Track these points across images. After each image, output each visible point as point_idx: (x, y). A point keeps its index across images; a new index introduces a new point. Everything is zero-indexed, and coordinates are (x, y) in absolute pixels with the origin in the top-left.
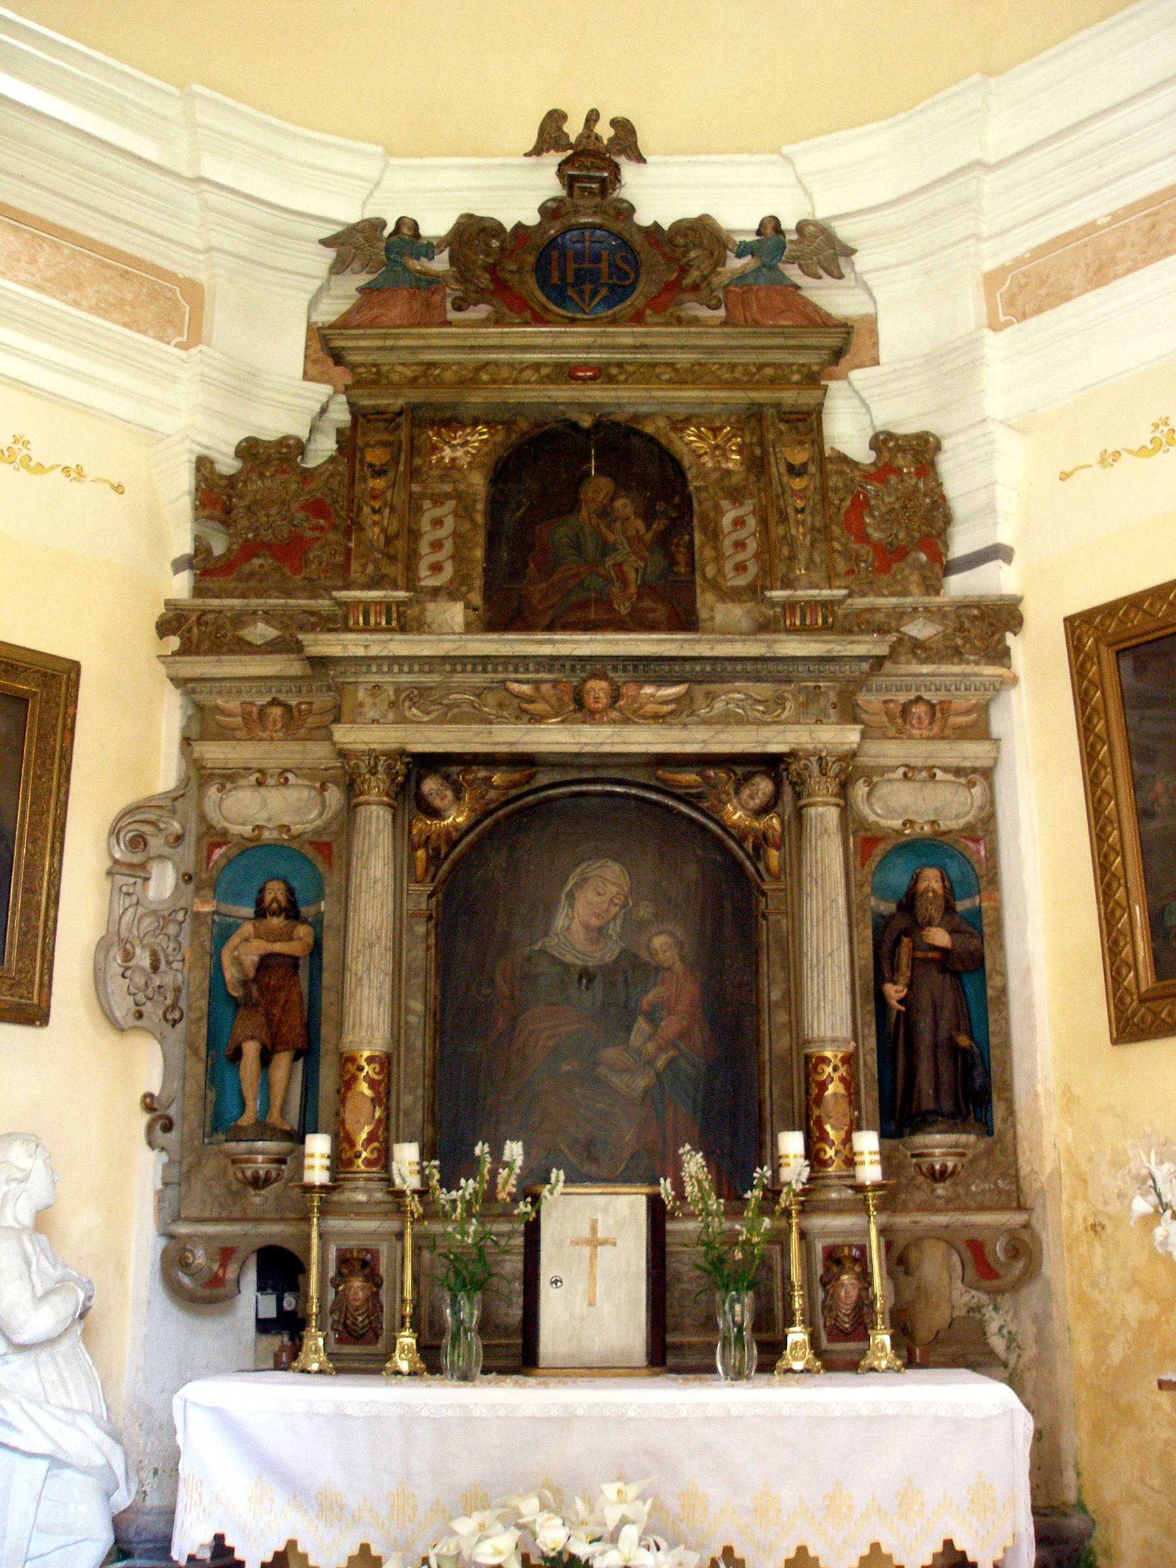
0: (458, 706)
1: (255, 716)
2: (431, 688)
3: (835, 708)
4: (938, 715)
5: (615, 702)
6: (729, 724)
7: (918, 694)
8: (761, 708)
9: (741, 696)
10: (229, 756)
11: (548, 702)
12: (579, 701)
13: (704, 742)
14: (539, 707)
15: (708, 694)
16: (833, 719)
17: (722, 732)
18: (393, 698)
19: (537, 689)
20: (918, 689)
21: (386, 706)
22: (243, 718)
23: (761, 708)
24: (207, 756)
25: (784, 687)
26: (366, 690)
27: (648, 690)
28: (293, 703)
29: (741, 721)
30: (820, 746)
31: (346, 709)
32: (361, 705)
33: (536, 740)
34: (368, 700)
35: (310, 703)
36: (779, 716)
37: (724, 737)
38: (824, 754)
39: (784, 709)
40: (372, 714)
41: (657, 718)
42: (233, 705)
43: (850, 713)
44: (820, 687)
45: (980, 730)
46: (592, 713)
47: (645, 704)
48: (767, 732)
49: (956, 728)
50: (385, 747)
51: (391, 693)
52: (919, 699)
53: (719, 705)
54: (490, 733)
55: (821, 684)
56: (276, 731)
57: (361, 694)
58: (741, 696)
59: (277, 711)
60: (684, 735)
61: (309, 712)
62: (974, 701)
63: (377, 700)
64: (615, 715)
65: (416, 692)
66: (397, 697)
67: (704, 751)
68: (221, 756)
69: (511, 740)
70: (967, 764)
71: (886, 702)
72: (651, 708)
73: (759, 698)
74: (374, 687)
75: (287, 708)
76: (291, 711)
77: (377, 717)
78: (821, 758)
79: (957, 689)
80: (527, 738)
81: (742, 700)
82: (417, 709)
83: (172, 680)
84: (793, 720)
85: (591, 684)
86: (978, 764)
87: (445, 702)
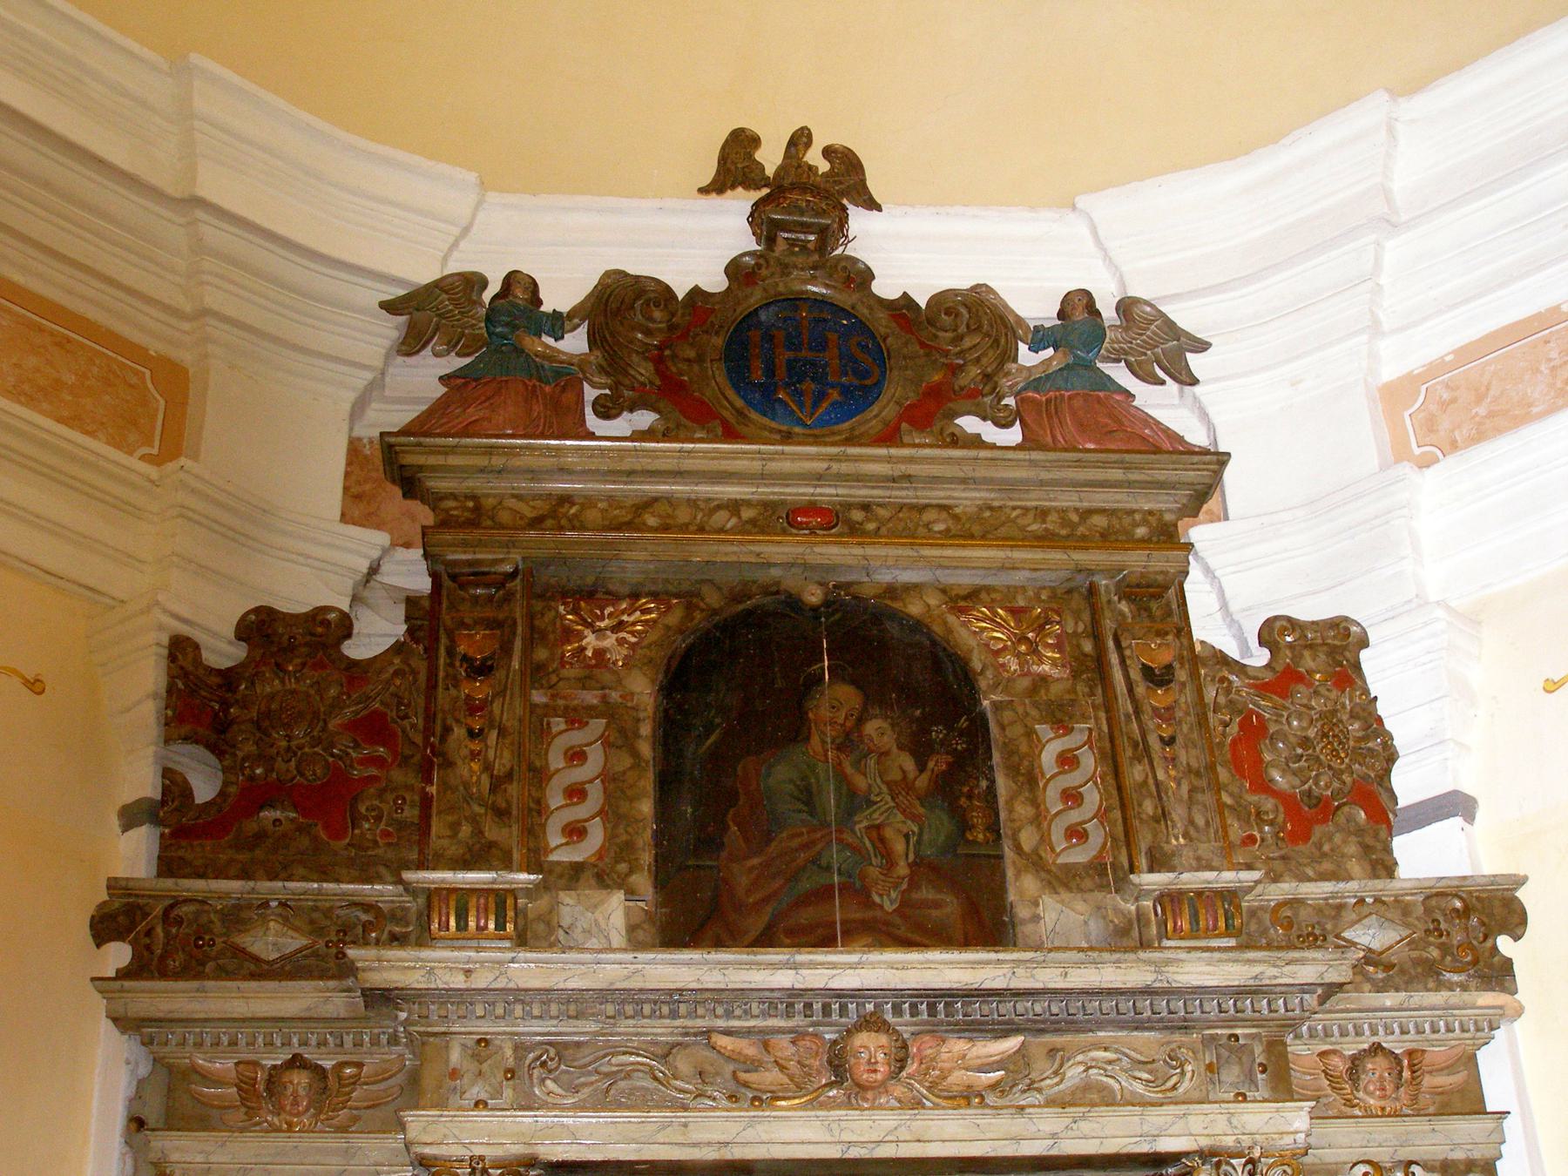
0: (628, 1076)
1: (261, 1087)
2: (578, 1044)
3: (1263, 1072)
4: (1406, 1074)
5: (902, 1068)
6: (1093, 1105)
7: (1375, 1039)
8: (1145, 1076)
9: (1109, 1055)
10: (213, 1159)
11: (782, 1068)
12: (838, 1065)
13: (1054, 1136)
14: (770, 1077)
15: (1052, 1052)
16: (1263, 1092)
17: (1084, 1117)
18: (511, 1062)
19: (766, 1046)
20: (1374, 1033)
21: (500, 1076)
22: (240, 1089)
23: (1145, 1076)
24: (175, 1157)
25: (1177, 1037)
26: (464, 1046)
27: (957, 1046)
28: (328, 1064)
29: (1108, 1099)
30: (1246, 1141)
31: (429, 1080)
32: (454, 1074)
33: (765, 1137)
34: (469, 1066)
35: (360, 1065)
36: (1174, 1088)
37: (1085, 1127)
38: (1256, 1153)
39: (1183, 1073)
40: (477, 1091)
41: (968, 1097)
42: (223, 1065)
44: (1236, 1037)
46: (862, 1087)
47: (950, 1071)
48: (1157, 1118)
49: (1437, 1092)
50: (499, 1152)
51: (509, 1052)
52: (1377, 1049)
53: (1074, 1073)
54: (685, 1125)
55: (1238, 1031)
56: (298, 1114)
57: (455, 1056)
58: (1109, 1055)
59: (300, 1080)
60: (1018, 1125)
61: (355, 1081)
62: (1460, 1049)
63: (485, 1067)
64: (899, 1091)
65: (552, 1052)
66: (519, 1059)
67: (1054, 1152)
68: (200, 1158)
69: (723, 1138)
70: (1459, 1155)
71: (1322, 1054)
72: (958, 1078)
73: (1139, 1057)
74: (479, 1041)
75: (320, 1072)
76: (326, 1077)
77: (483, 1096)
78: (1251, 1161)
79: (1435, 1030)
80: (750, 1134)
81: (1110, 1062)
82: (554, 1080)
83: (115, 1020)
84: (1196, 1095)
85: (864, 1039)
86: (1476, 1155)
87: (605, 1069)
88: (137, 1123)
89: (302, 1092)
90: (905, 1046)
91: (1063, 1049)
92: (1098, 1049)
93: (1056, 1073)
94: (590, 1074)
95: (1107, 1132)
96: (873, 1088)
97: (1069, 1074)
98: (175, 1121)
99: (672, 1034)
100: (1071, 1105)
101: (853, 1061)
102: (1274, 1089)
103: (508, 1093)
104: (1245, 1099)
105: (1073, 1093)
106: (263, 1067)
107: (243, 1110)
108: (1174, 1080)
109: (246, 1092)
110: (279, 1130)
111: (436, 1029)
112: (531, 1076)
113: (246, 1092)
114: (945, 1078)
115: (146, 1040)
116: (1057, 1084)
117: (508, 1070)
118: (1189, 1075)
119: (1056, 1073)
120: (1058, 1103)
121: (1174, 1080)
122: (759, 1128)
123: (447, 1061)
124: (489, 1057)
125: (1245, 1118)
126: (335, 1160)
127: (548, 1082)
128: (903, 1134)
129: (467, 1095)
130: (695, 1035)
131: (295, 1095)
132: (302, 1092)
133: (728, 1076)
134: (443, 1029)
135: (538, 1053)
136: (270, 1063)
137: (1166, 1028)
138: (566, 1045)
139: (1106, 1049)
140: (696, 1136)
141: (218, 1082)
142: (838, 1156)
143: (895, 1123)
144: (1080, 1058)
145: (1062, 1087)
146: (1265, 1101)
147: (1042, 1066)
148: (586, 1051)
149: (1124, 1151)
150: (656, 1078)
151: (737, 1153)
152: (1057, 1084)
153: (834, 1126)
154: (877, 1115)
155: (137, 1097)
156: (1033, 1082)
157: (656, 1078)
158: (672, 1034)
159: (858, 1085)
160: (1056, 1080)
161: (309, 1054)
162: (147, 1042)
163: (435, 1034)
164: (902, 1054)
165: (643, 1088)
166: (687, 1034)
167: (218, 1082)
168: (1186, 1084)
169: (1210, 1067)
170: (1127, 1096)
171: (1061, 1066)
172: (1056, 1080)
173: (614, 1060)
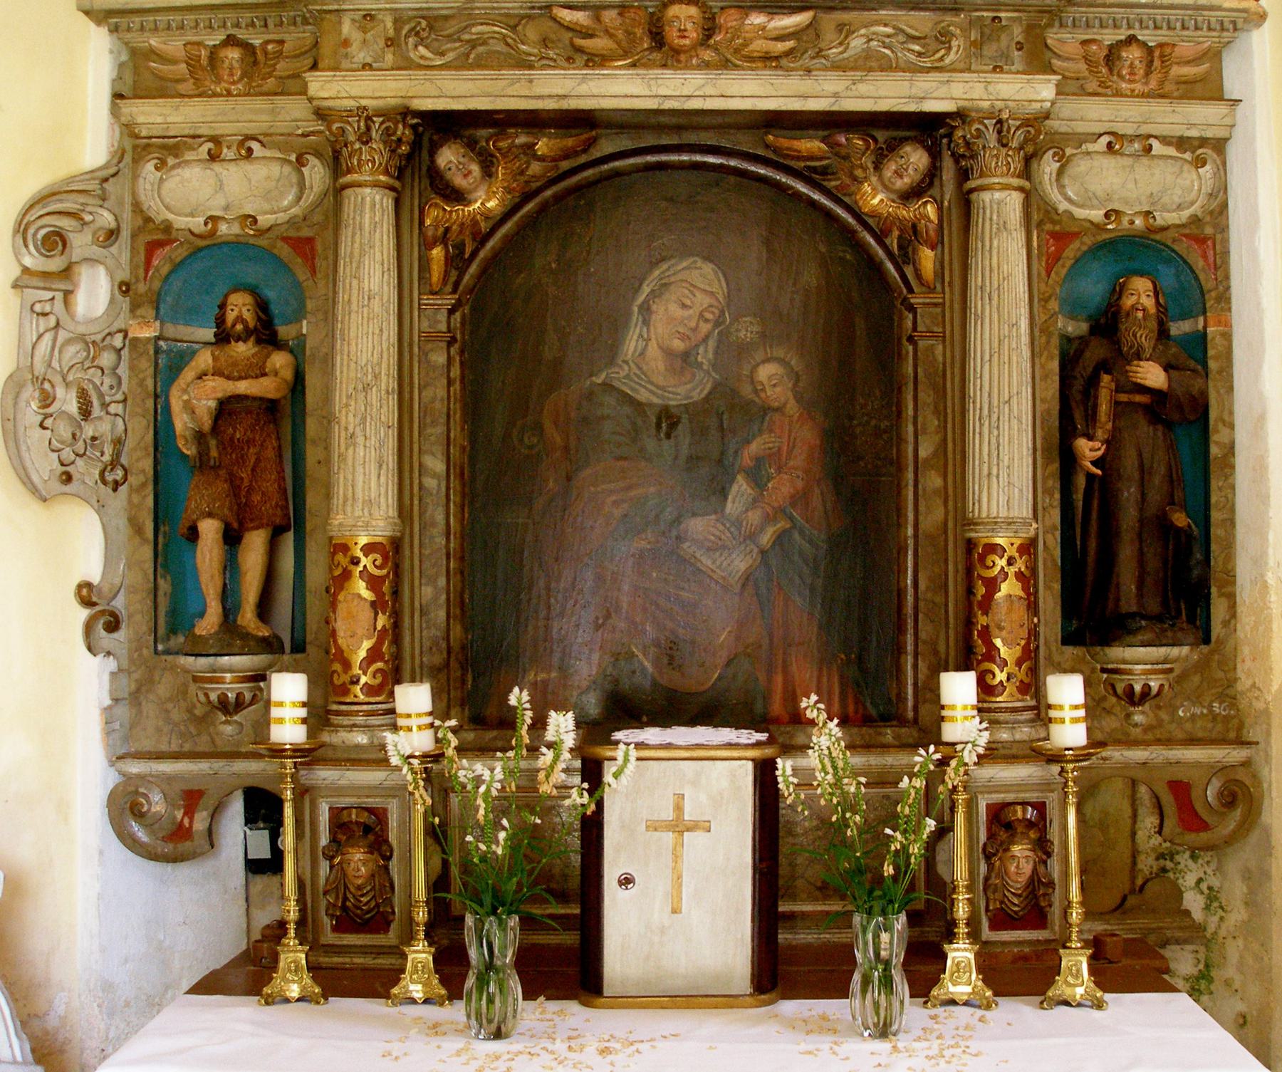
0: (484, 43)
1: (204, 62)
2: (446, 18)
3: (1019, 50)
4: (1157, 63)
5: (709, 37)
6: (870, 70)
7: (1131, 32)
8: (917, 48)
9: (889, 30)
10: (169, 120)
11: (611, 36)
12: (658, 38)
13: (836, 95)
14: (599, 44)
15: (840, 27)
16: (1018, 66)
17: (861, 81)
18: (391, 33)
19: (598, 19)
20: (1129, 27)
21: (382, 43)
22: (188, 64)
23: (917, 48)
24: (141, 119)
25: (949, 18)
26: (354, 21)
27: (757, 19)
28: (257, 42)
29: (887, 66)
30: (999, 104)
31: (326, 50)
32: (346, 43)
33: (595, 91)
34: (356, 36)
35: (282, 42)
36: (941, 59)
37: (863, 88)
38: (1005, 116)
39: (950, 48)
40: (362, 56)
41: (769, 60)
42: (174, 46)
43: (1038, 58)
44: (1000, 18)
45: (1208, 88)
46: (677, 52)
47: (751, 40)
48: (925, 83)
49: (1180, 82)
50: (380, 103)
51: (389, 25)
52: (1131, 40)
53: (857, 43)
54: (531, 81)
55: (1002, 15)
56: (234, 83)
57: (347, 28)
58: (889, 30)
59: (233, 54)
60: (805, 85)
61: (279, 55)
62: (1206, 45)
63: (369, 36)
64: (707, 55)
65: (424, 23)
66: (397, 30)
67: (835, 108)
68: (159, 120)
69: (561, 92)
70: (1194, 133)
71: (1085, 43)
72: (759, 46)
73: (917, 34)
74: (365, 16)
75: (247, 47)
76: (254, 53)
77: (369, 60)
78: (1000, 122)
79: (1184, 28)
80: (583, 89)
81: (888, 36)
82: (426, 47)
83: (87, 13)
84: (962, 66)
85: (675, 10)
86: (1209, 134)
87: (466, 37)
88: (118, 96)
89: (236, 65)
90: (713, 19)
91: (850, 25)
92: (879, 25)
93: (841, 44)
94: (455, 41)
95: (882, 93)
96: (685, 52)
97: (852, 45)
98: (140, 93)
99: (521, 8)
100: (853, 69)
101: (667, 28)
102: (1029, 64)
103: (389, 57)
104: (1002, 71)
105: (856, 61)
106: (205, 47)
107: (192, 81)
108: (942, 52)
109: (193, 66)
110: (220, 95)
111: (331, 7)
112: (406, 43)
113: (193, 66)
114: (746, 46)
115: (112, 28)
116: (841, 53)
117: (389, 39)
118: (954, 49)
119: (841, 44)
120: (839, 67)
121: (942, 52)
122: (591, 84)
123: (340, 33)
124: (372, 28)
125: (1000, 86)
126: (264, 117)
127: (420, 48)
128: (709, 90)
129: (355, 60)
130: (540, 8)
131: (231, 68)
132: (236, 65)
133: (567, 42)
134: (336, 7)
135: (413, 24)
136: (212, 43)
137: (939, 9)
138: (436, 18)
139: (886, 25)
140: (538, 90)
141: (174, 61)
142: (655, 107)
143: (703, 82)
144: (863, 31)
145: (845, 55)
146: (1018, 72)
147: (829, 34)
148: (453, 22)
149: (895, 109)
150: (508, 44)
151: (573, 104)
152: (844, 52)
153: (652, 82)
154: (689, 75)
155: (119, 79)
156: (821, 50)
157: (508, 44)
158: (521, 8)
159: (672, 49)
160: (840, 49)
161: (242, 35)
162: (114, 30)
163: (330, 11)
164: (710, 25)
165: (498, 52)
166: (533, 8)
167: (174, 61)
168: (952, 57)
169: (974, 43)
170: (902, 64)
171: (846, 37)
172: (840, 49)
173: (474, 30)
